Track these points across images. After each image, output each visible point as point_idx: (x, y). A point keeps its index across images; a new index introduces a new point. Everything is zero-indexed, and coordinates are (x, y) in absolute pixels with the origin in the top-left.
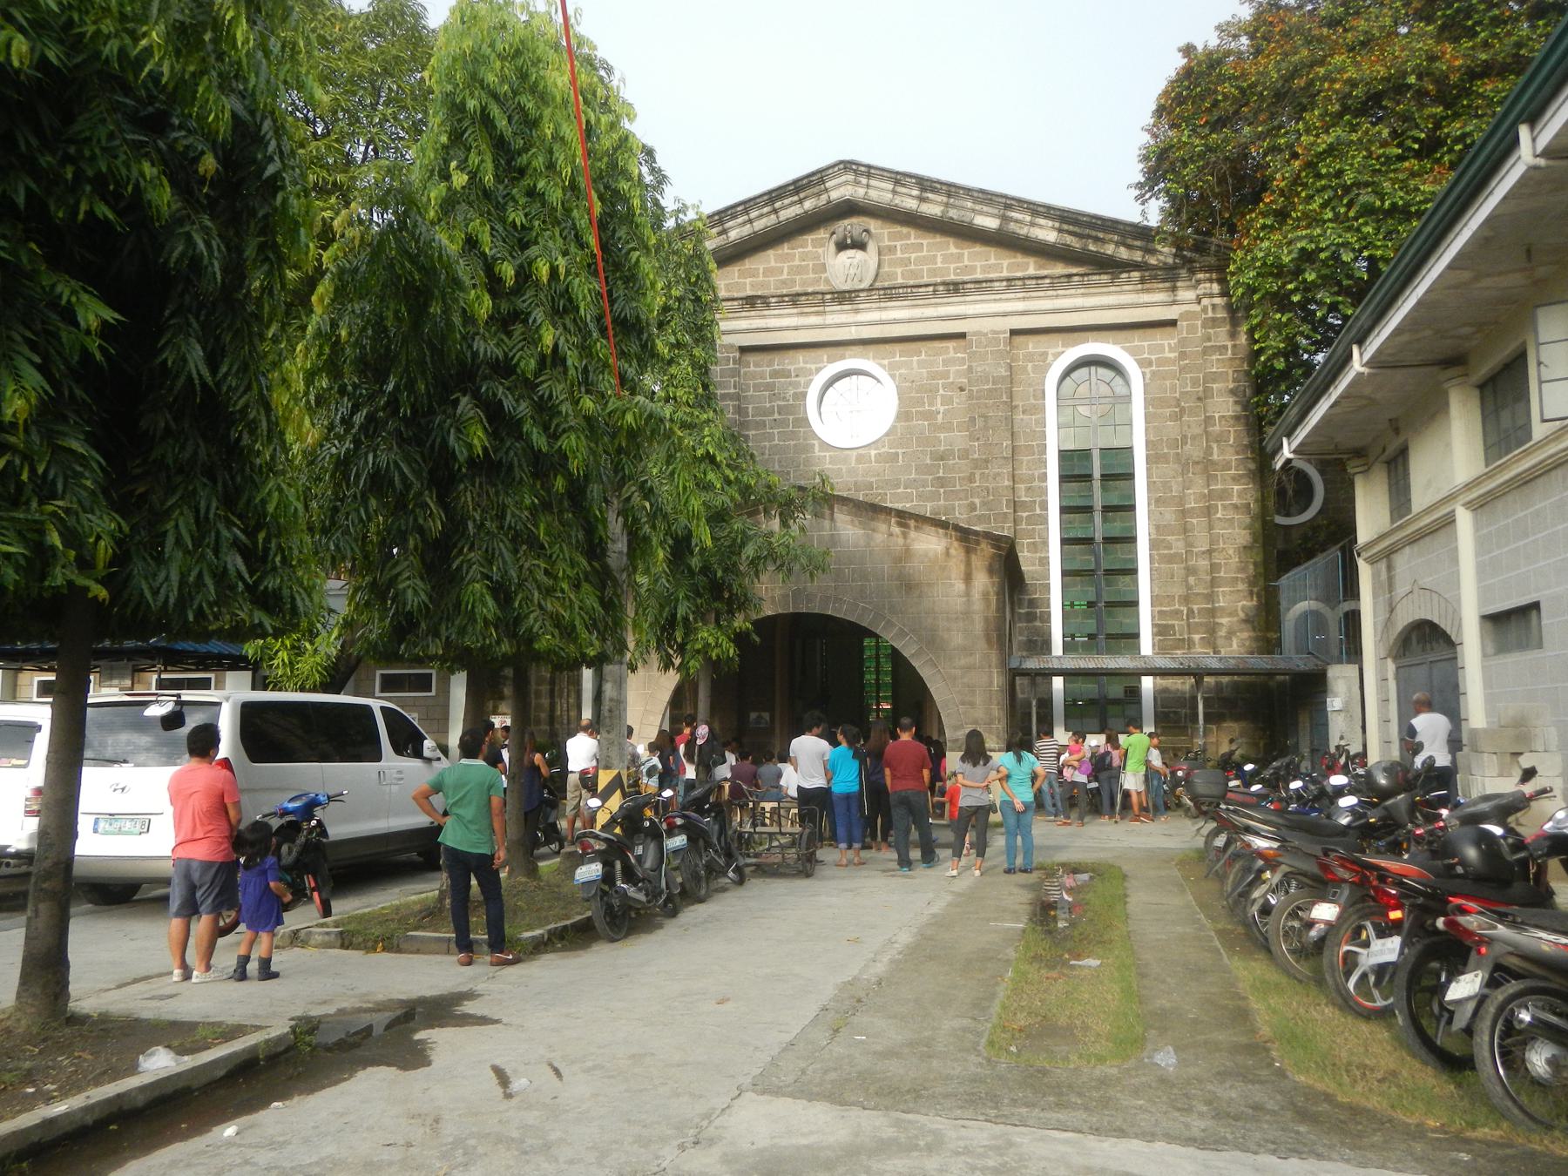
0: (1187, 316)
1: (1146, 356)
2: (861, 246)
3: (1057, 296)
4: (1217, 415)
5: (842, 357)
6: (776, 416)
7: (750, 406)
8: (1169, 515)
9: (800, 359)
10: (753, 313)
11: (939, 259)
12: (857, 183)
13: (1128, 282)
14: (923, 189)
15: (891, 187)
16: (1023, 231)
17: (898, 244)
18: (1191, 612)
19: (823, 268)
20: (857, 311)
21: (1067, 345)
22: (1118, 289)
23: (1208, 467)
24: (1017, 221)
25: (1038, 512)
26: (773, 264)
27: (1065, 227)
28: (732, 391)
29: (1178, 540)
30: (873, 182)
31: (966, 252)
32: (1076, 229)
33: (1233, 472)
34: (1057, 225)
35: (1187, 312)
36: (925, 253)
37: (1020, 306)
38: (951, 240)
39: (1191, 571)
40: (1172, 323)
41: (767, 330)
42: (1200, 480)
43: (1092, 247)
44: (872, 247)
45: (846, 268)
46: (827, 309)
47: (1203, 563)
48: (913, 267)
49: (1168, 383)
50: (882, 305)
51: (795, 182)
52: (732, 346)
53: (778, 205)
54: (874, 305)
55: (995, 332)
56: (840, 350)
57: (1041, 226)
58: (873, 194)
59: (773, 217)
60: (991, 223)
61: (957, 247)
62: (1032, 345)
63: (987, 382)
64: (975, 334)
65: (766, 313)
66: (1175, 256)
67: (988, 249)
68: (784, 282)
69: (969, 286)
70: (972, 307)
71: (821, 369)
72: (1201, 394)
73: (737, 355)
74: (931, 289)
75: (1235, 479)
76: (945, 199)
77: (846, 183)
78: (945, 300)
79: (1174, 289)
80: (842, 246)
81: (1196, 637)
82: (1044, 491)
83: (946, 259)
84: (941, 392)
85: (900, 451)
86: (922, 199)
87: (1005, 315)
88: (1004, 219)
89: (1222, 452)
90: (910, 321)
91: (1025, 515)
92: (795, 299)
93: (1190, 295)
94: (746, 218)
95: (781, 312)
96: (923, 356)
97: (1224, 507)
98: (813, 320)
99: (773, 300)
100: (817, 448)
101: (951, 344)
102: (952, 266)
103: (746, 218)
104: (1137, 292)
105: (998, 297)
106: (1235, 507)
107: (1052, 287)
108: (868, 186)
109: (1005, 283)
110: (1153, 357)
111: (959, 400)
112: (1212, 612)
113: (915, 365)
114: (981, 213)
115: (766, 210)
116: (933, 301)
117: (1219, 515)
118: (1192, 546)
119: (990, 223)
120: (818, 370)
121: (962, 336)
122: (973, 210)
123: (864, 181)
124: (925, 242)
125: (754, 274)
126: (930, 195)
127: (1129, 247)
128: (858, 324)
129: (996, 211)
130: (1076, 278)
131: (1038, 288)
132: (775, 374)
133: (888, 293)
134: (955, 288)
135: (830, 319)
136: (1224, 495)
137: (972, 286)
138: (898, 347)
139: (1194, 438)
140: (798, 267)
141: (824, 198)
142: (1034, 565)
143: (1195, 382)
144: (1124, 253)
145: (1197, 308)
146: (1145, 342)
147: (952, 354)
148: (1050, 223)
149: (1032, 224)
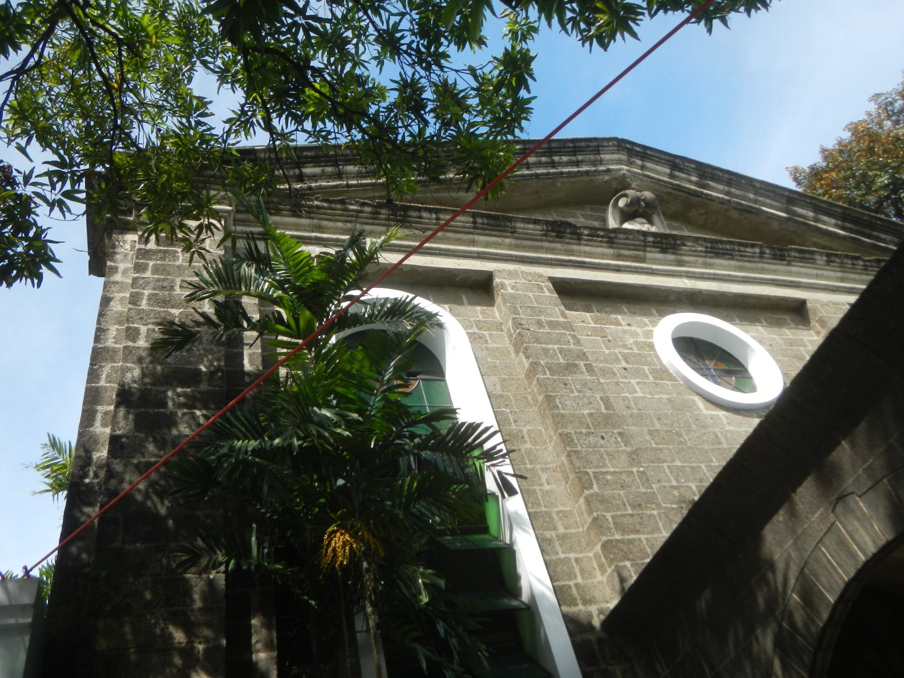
10: (558, 246)
12: (630, 164)
15: (668, 171)
20: (680, 263)
27: (848, 225)
34: (840, 223)
46: (649, 255)
50: (709, 260)
57: (824, 223)
65: (575, 247)
76: (727, 188)
77: (619, 162)
78: (772, 267)
95: (594, 250)
99: (586, 232)
105: (820, 272)
115: (544, 159)
116: (760, 265)
123: (639, 162)
126: (712, 184)
137: (797, 255)
148: (833, 221)
149: (817, 220)
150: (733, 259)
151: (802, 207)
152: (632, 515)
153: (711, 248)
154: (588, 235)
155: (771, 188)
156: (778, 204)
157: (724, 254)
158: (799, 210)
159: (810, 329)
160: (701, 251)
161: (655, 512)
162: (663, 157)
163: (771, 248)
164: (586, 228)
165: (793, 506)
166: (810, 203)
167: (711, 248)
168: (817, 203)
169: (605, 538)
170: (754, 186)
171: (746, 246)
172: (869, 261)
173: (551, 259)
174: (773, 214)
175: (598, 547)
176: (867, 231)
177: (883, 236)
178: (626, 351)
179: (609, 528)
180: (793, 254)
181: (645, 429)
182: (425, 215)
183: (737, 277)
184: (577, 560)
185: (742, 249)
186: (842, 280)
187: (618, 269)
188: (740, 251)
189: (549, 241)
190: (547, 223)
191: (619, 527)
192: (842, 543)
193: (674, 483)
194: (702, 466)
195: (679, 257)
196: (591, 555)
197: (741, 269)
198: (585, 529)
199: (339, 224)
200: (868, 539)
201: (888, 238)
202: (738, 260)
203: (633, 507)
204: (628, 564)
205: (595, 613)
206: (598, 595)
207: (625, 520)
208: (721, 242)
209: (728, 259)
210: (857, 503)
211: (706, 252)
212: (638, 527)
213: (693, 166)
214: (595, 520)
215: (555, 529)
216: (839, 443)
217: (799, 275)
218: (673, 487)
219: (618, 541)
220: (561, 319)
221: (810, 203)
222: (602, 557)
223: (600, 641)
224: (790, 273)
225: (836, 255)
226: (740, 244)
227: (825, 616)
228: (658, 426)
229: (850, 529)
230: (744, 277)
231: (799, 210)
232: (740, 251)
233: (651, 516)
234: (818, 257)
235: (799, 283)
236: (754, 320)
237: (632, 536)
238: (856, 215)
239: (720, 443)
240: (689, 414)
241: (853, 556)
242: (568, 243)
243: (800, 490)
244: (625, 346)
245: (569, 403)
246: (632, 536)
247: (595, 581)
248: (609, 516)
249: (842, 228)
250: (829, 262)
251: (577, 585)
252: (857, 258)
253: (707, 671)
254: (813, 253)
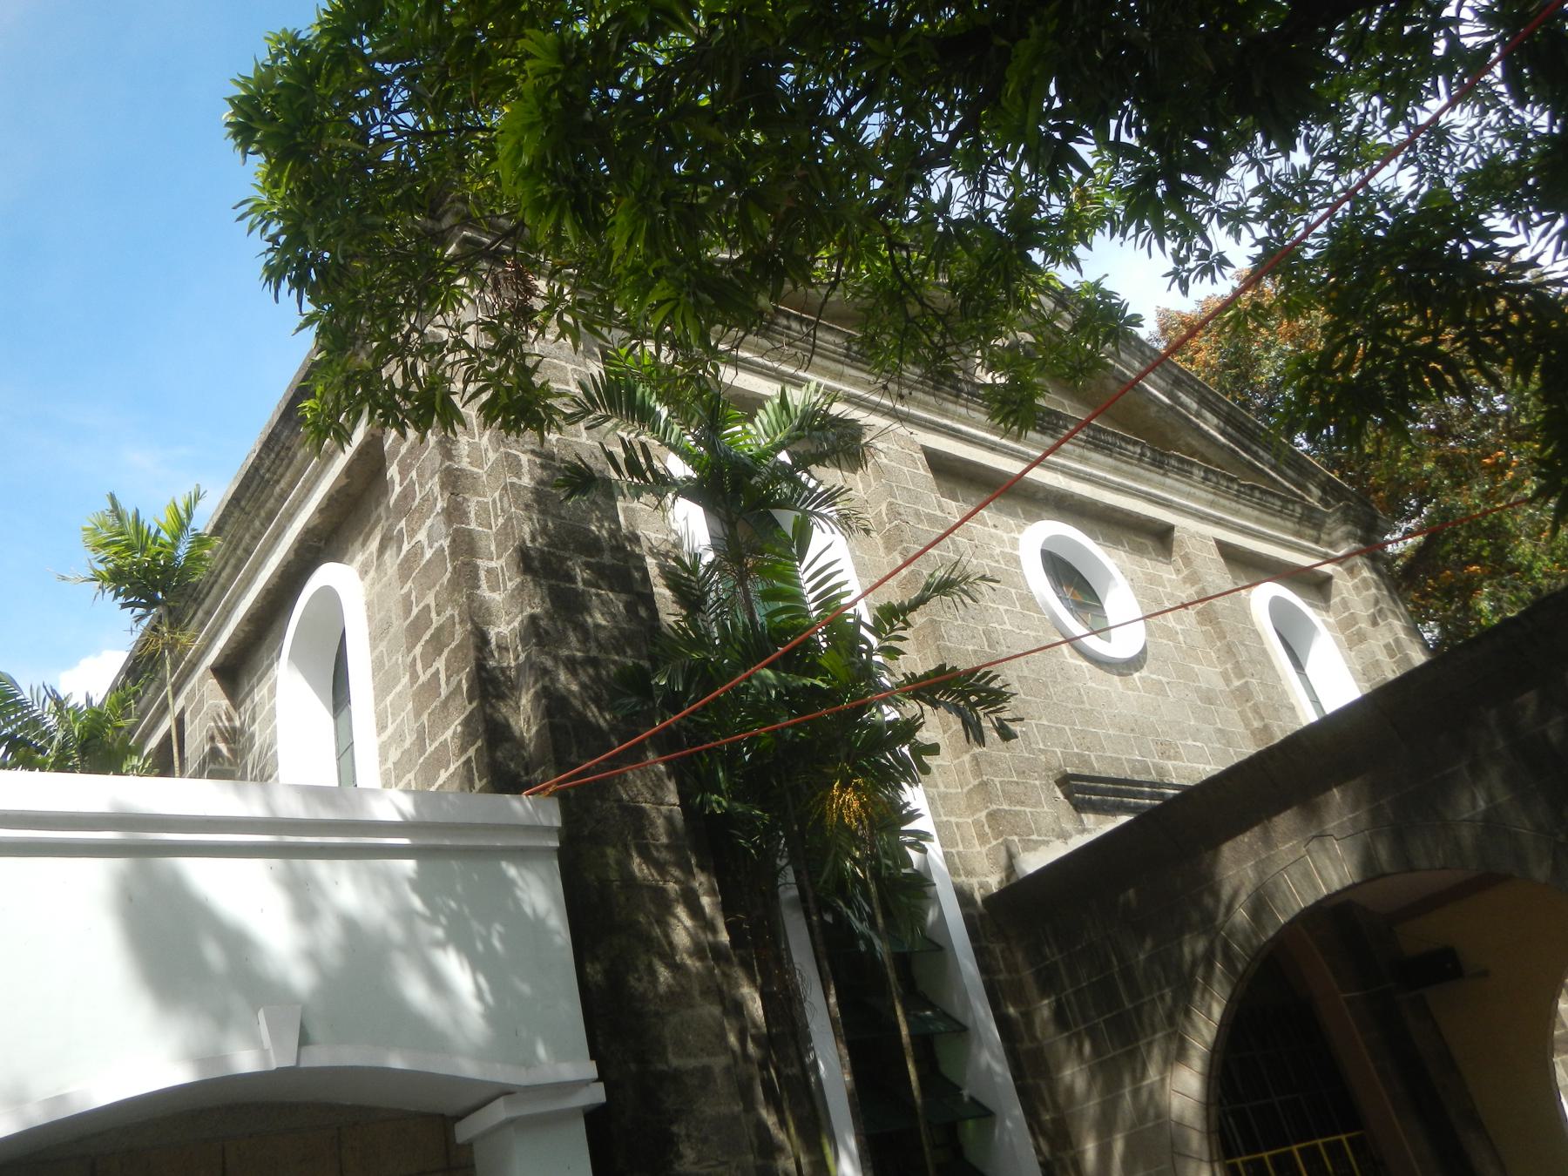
10: (931, 400)
27: (1229, 429)
34: (1222, 424)
57: (1206, 421)
65: (951, 406)
105: (1193, 490)
148: (1215, 421)
149: (1198, 415)
150: (1110, 456)
152: (1017, 783)
153: (1093, 438)
154: (968, 393)
156: (1162, 384)
157: (1103, 448)
158: (1184, 398)
159: (1170, 563)
160: (1081, 440)
161: (1037, 783)
163: (1153, 450)
165: (1266, 831)
166: (1197, 391)
167: (1093, 438)
168: (1205, 392)
169: (994, 807)
170: (1143, 353)
171: (1128, 441)
172: (1244, 486)
173: (926, 420)
174: (1155, 396)
175: (984, 813)
176: (1247, 442)
177: (1261, 453)
178: (994, 564)
179: (998, 796)
180: (1173, 462)
181: (1015, 674)
182: (795, 325)
183: (1112, 482)
184: (958, 825)
185: (1123, 444)
186: (1212, 504)
187: (993, 448)
188: (1120, 447)
189: (924, 392)
191: (1008, 796)
192: (1307, 875)
193: (1042, 746)
194: (1067, 728)
196: (970, 821)
197: (1116, 471)
198: (965, 790)
200: (1335, 878)
201: (1266, 456)
202: (1115, 459)
203: (1018, 774)
204: (1016, 838)
205: (976, 887)
206: (978, 867)
207: (1012, 788)
208: (1105, 431)
209: (1106, 455)
210: (1333, 844)
211: (1085, 442)
212: (1023, 798)
214: (984, 784)
215: (936, 786)
216: (1330, 789)
217: (1172, 490)
218: (1040, 750)
219: (1006, 811)
220: (938, 513)
221: (1197, 391)
222: (986, 826)
223: (981, 916)
224: (1162, 486)
225: (1214, 472)
226: (1123, 439)
227: (1271, 933)
228: (1026, 673)
229: (1319, 864)
230: (1119, 484)
231: (1184, 398)
232: (1120, 447)
233: (1035, 786)
234: (1195, 471)
235: (1171, 501)
236: (1116, 542)
237: (1018, 808)
238: (1242, 419)
239: (1083, 702)
240: (1054, 660)
241: (1315, 887)
242: (944, 399)
243: (1276, 819)
244: (992, 556)
245: (953, 633)
246: (1018, 808)
247: (974, 850)
248: (997, 780)
249: (1223, 433)
250: (1205, 479)
251: (959, 853)
252: (1232, 480)
253: (1115, 963)
254: (1192, 464)
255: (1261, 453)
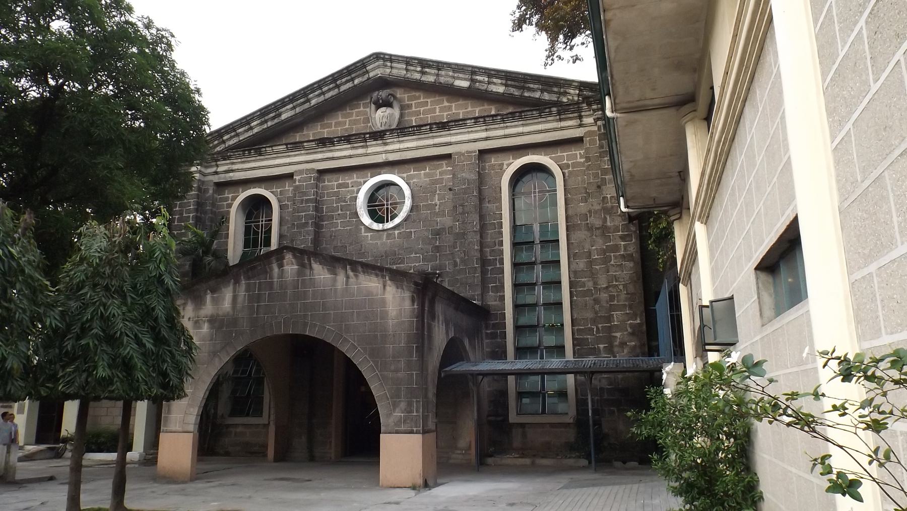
0: (589, 133)
1: (565, 161)
2: (388, 104)
3: (507, 127)
4: (609, 196)
5: (380, 174)
6: (340, 212)
7: (325, 207)
8: (581, 264)
9: (355, 177)
10: (325, 149)
11: (438, 110)
13: (550, 114)
14: (423, 67)
16: (484, 87)
17: (413, 102)
18: (598, 328)
19: (367, 120)
20: (386, 144)
21: (515, 158)
22: (544, 119)
23: (604, 230)
24: (480, 82)
25: (498, 266)
26: (340, 119)
27: (509, 82)
28: (312, 197)
29: (589, 281)
30: (394, 65)
31: (453, 105)
32: (516, 84)
33: (621, 233)
34: (504, 82)
35: (589, 132)
36: (429, 107)
37: (484, 135)
38: (445, 98)
39: (597, 301)
40: (578, 141)
41: (333, 159)
42: (600, 241)
43: (526, 94)
44: (395, 104)
45: (381, 117)
46: (368, 144)
47: (604, 296)
48: (422, 116)
49: (579, 178)
50: (401, 139)
51: (347, 68)
52: (313, 169)
53: (338, 82)
54: (395, 140)
55: (468, 152)
56: (378, 170)
57: (495, 84)
58: (395, 71)
59: (336, 91)
60: (465, 84)
61: (448, 102)
62: (494, 160)
63: (464, 184)
64: (457, 153)
66: (579, 95)
67: (466, 102)
68: (346, 130)
69: (451, 124)
70: (455, 137)
71: (366, 181)
72: (599, 184)
73: (316, 175)
74: (428, 127)
75: (623, 238)
76: (436, 71)
77: (378, 67)
78: (438, 134)
79: (580, 117)
80: (378, 106)
81: (601, 346)
82: (502, 252)
83: (442, 109)
84: (438, 192)
85: (412, 230)
86: (423, 73)
87: (475, 141)
88: (473, 81)
89: (613, 220)
90: (417, 148)
91: (490, 268)
92: (348, 139)
93: (590, 120)
94: (320, 91)
96: (427, 171)
97: (615, 257)
98: (360, 151)
100: (363, 230)
101: (444, 162)
102: (445, 114)
103: (320, 91)
104: (557, 121)
105: (470, 130)
106: (623, 256)
107: (503, 121)
108: (391, 67)
109: (473, 121)
110: (570, 162)
111: (449, 196)
112: (610, 329)
113: (422, 175)
114: (459, 78)
115: (331, 86)
116: (431, 135)
117: (612, 262)
118: (598, 285)
119: (463, 83)
120: (365, 182)
121: (448, 156)
122: (454, 77)
124: (429, 100)
125: (330, 126)
126: (427, 70)
127: (550, 92)
128: (386, 152)
129: (467, 76)
130: (517, 114)
131: (494, 122)
132: (339, 186)
133: (402, 130)
134: (443, 126)
135: (370, 150)
136: (616, 248)
138: (412, 167)
139: (596, 212)
140: (354, 120)
141: (366, 77)
142: (496, 301)
143: (596, 176)
144: (546, 96)
145: (596, 128)
146: (564, 154)
147: (445, 168)
148: (499, 81)
149: (489, 83)
151: (480, 75)
155: (462, 67)
162: (400, 59)
164: (335, 138)
177: (532, 86)
182: (267, 149)
190: (316, 140)
195: (384, 141)
199: (239, 160)
213: (416, 61)
221: (484, 73)
255: (532, 86)
